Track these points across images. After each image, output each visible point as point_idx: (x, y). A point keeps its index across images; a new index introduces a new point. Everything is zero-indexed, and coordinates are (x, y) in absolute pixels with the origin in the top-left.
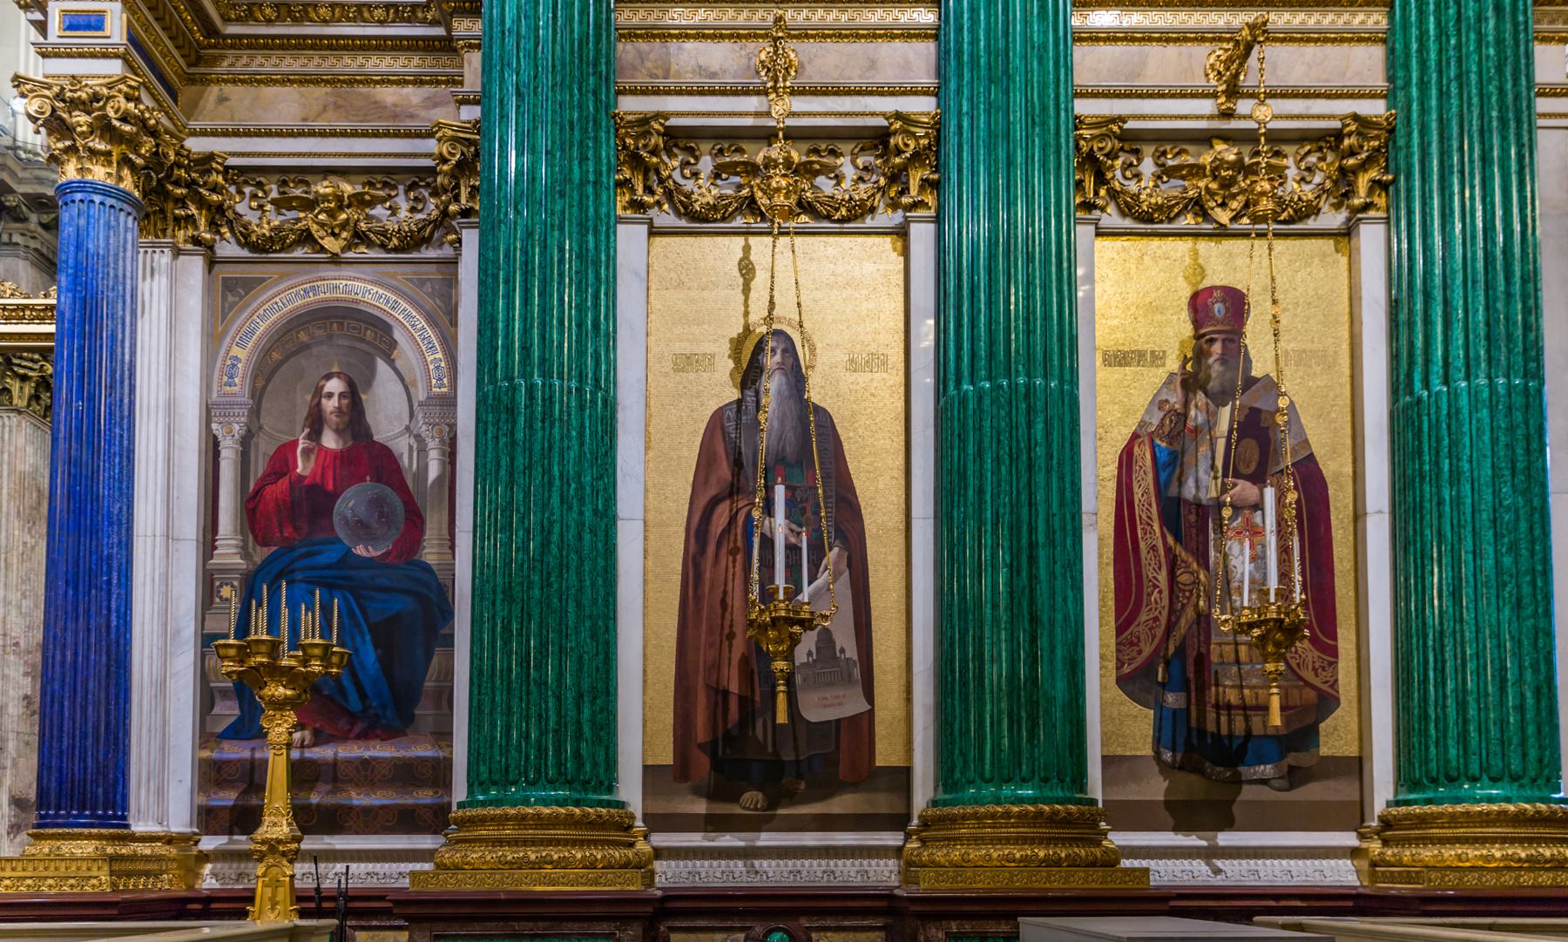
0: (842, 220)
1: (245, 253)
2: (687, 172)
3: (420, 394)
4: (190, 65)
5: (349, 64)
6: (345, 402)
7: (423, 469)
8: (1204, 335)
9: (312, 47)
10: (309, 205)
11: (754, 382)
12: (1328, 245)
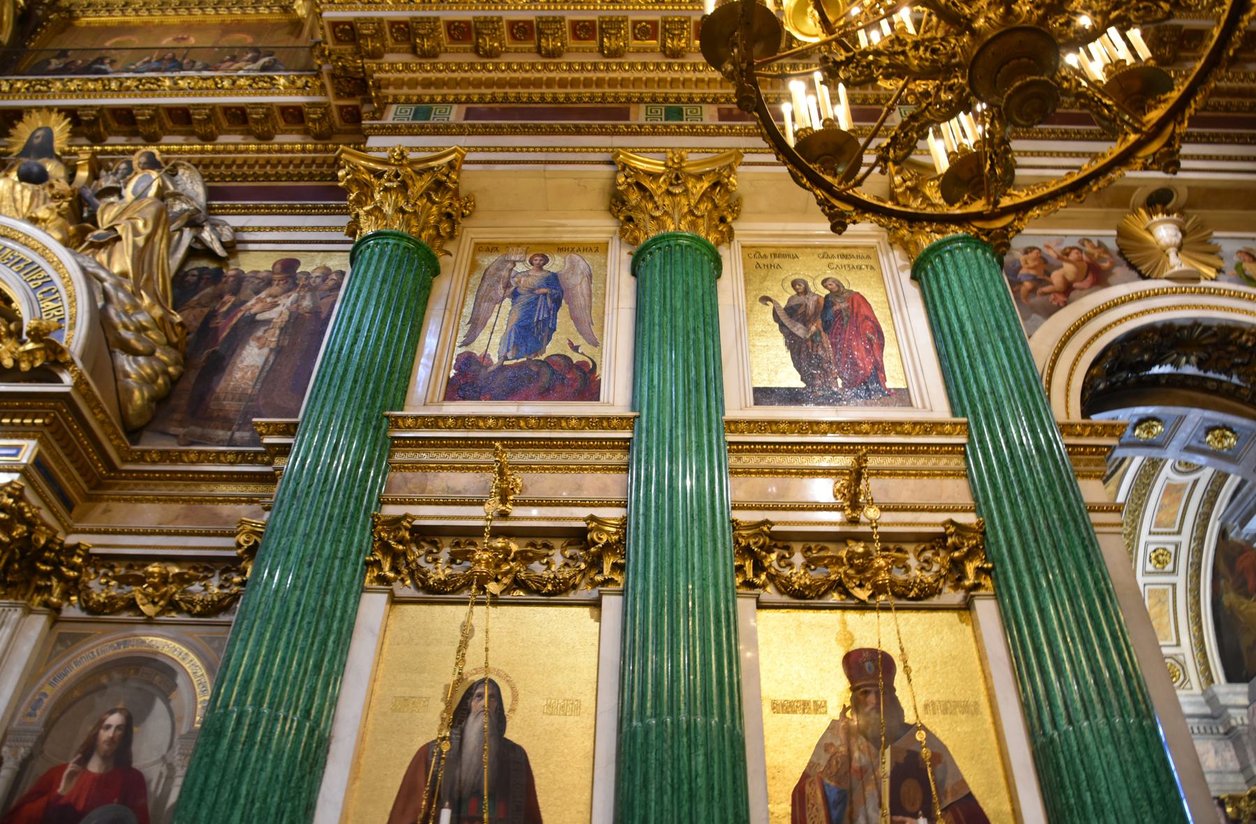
0: (549, 594)
1: (84, 615)
2: (429, 558)
3: (183, 729)
4: (91, 489)
5: (204, 490)
6: (119, 733)
7: (166, 794)
8: (858, 688)
9: (180, 479)
10: (140, 581)
11: (460, 722)
12: (952, 617)
